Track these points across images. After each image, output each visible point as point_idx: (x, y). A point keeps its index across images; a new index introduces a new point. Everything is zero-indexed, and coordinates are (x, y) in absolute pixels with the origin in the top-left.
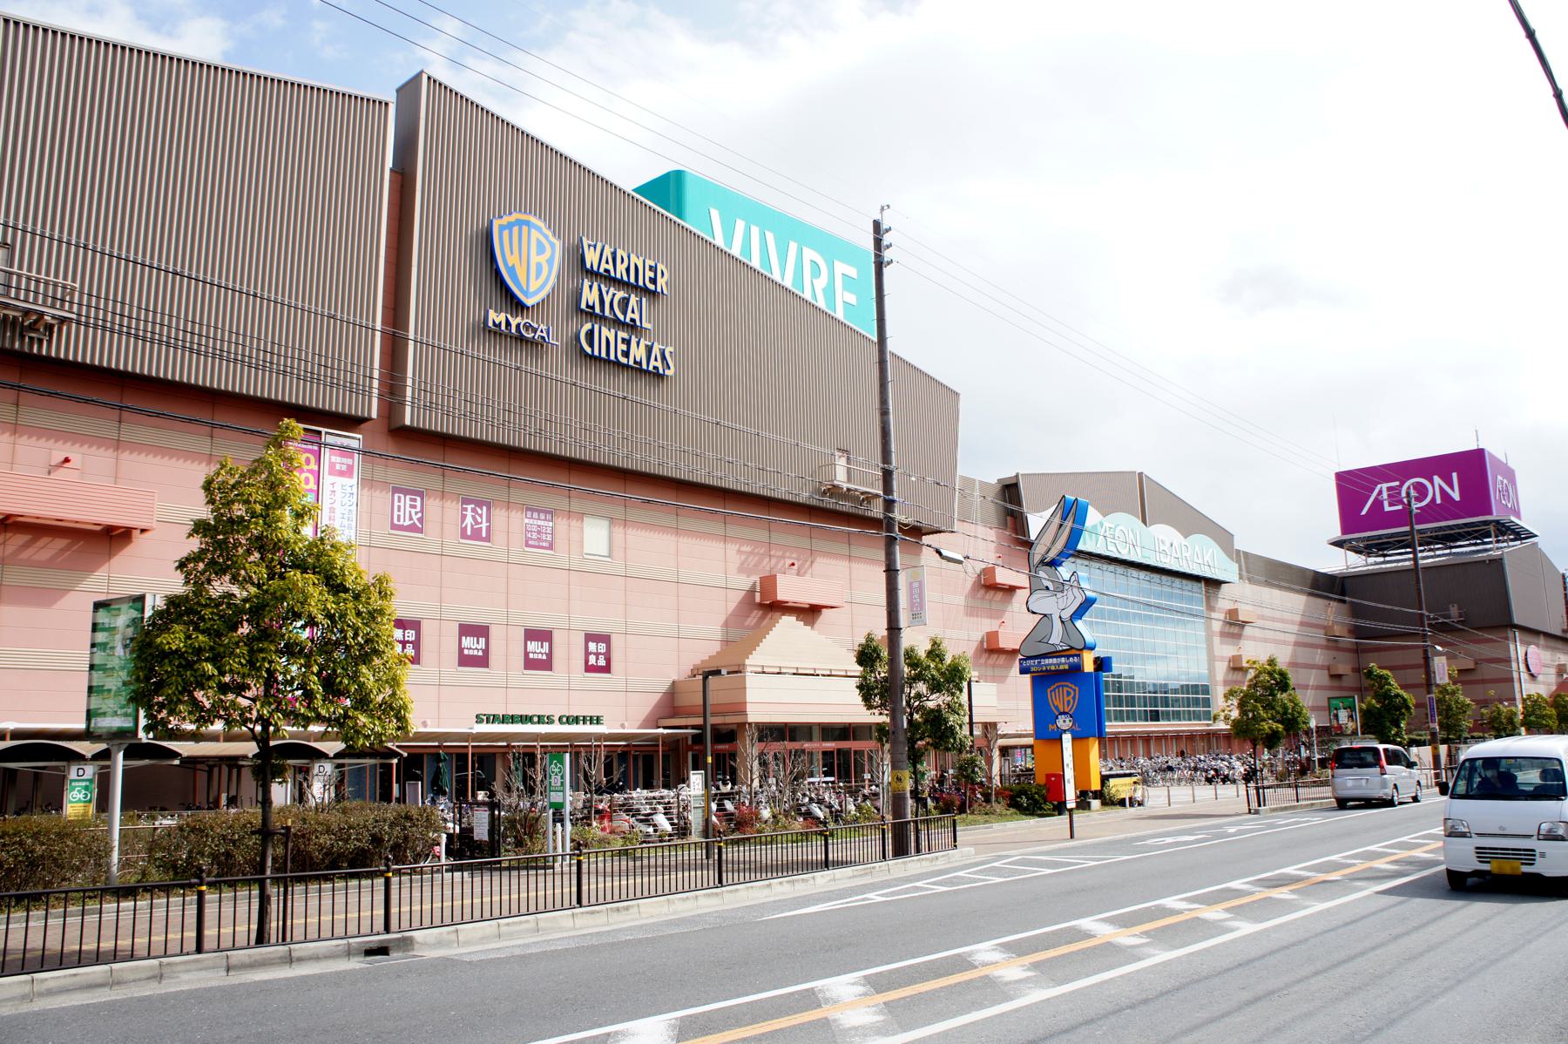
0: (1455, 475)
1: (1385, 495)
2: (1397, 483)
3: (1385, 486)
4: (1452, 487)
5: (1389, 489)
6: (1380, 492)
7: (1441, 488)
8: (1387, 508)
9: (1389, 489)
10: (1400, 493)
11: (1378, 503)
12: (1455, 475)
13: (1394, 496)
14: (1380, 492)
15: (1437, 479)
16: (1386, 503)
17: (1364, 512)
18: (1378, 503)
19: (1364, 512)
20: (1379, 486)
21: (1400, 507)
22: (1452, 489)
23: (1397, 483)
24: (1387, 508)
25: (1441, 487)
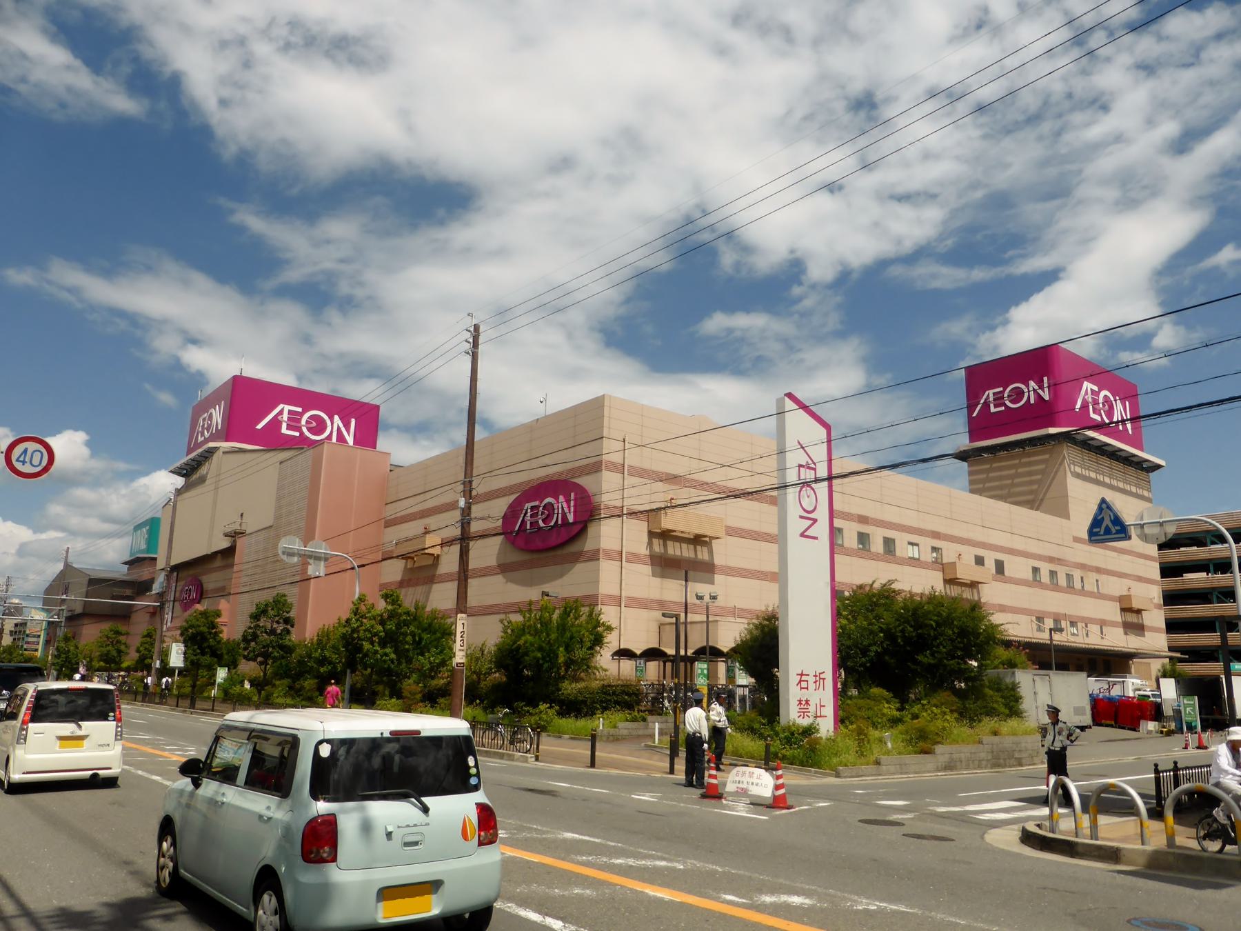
0: (353, 422)
1: (285, 416)
2: (300, 410)
3: (287, 408)
4: (348, 431)
5: (290, 412)
6: (281, 412)
7: (339, 429)
8: (284, 430)
9: (290, 412)
10: (299, 421)
11: (276, 423)
12: (353, 422)
13: (294, 422)
14: (281, 412)
15: (336, 418)
16: (284, 426)
17: (259, 427)
18: (276, 423)
19: (259, 427)
20: (281, 406)
21: (297, 434)
22: (348, 431)
23: (300, 410)
24: (284, 430)
25: (339, 429)
